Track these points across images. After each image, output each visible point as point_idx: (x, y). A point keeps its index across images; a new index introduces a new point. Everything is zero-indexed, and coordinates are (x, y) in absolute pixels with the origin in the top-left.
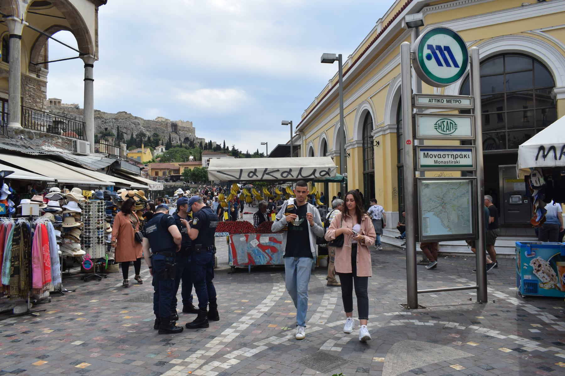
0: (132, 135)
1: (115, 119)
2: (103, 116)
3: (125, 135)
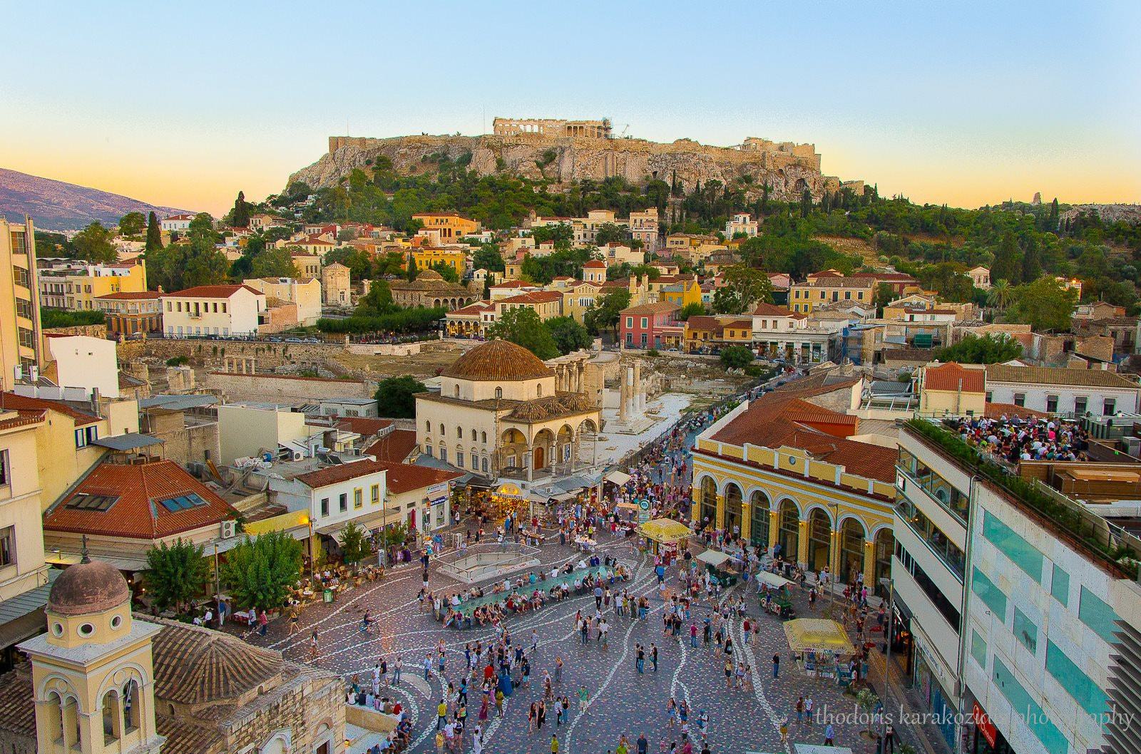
0: (698, 186)
2: (650, 148)
3: (685, 184)
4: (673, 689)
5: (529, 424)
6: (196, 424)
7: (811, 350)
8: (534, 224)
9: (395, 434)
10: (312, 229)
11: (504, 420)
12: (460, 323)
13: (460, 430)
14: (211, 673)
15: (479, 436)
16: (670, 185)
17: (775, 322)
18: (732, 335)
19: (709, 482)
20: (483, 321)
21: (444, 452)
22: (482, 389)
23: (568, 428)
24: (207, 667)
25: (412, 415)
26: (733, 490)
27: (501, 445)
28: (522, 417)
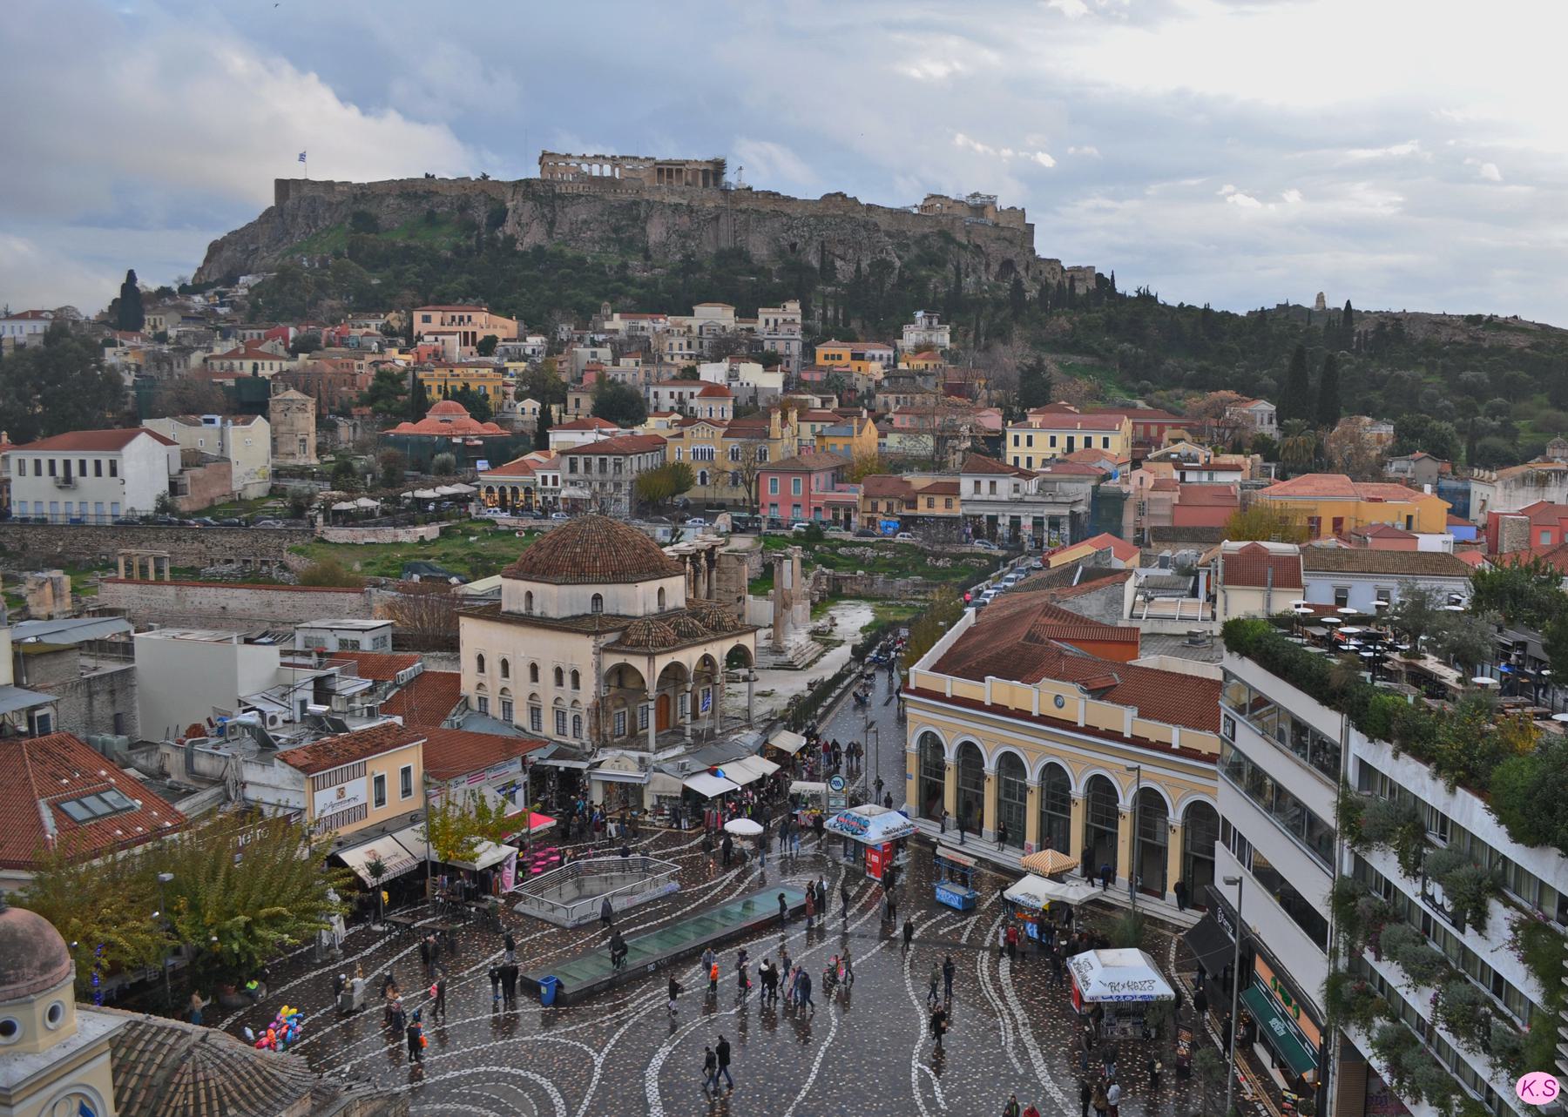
0: (858, 269)
1: (815, 216)
3: (838, 263)
4: (914, 1076)
5: (651, 656)
6: (95, 669)
7: (1046, 527)
8: (608, 325)
9: (422, 676)
10: (248, 332)
11: (608, 649)
12: (502, 489)
13: (534, 669)
14: (197, 1098)
15: (567, 679)
16: (816, 264)
17: (993, 484)
18: (930, 505)
19: (931, 744)
20: (540, 485)
21: (507, 707)
22: (556, 598)
23: (707, 659)
24: (191, 1088)
25: (451, 645)
26: (969, 753)
27: (603, 692)
28: (638, 643)
